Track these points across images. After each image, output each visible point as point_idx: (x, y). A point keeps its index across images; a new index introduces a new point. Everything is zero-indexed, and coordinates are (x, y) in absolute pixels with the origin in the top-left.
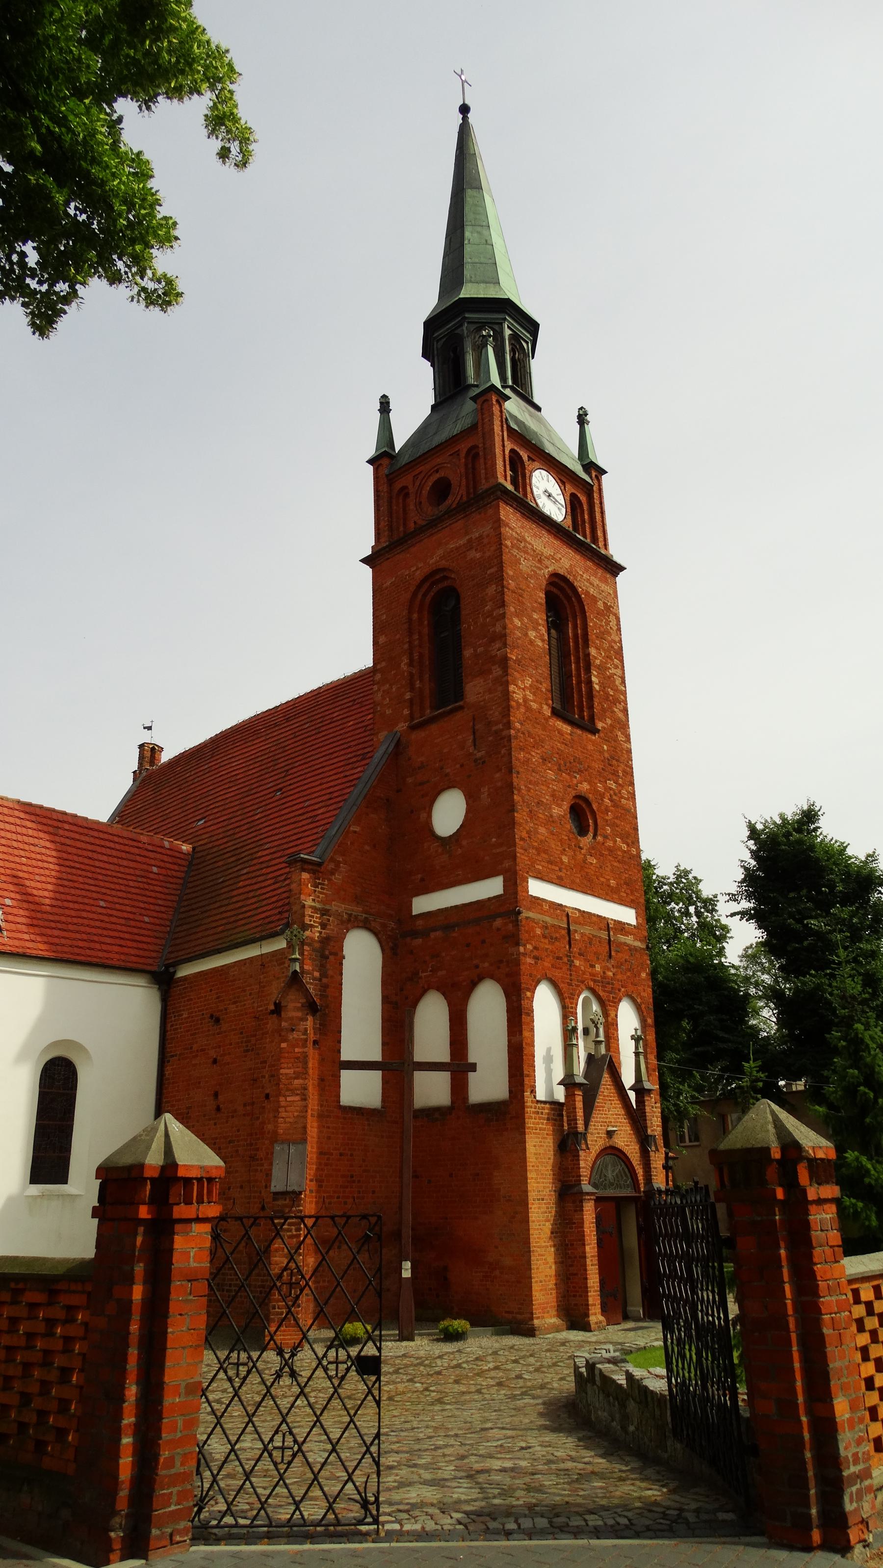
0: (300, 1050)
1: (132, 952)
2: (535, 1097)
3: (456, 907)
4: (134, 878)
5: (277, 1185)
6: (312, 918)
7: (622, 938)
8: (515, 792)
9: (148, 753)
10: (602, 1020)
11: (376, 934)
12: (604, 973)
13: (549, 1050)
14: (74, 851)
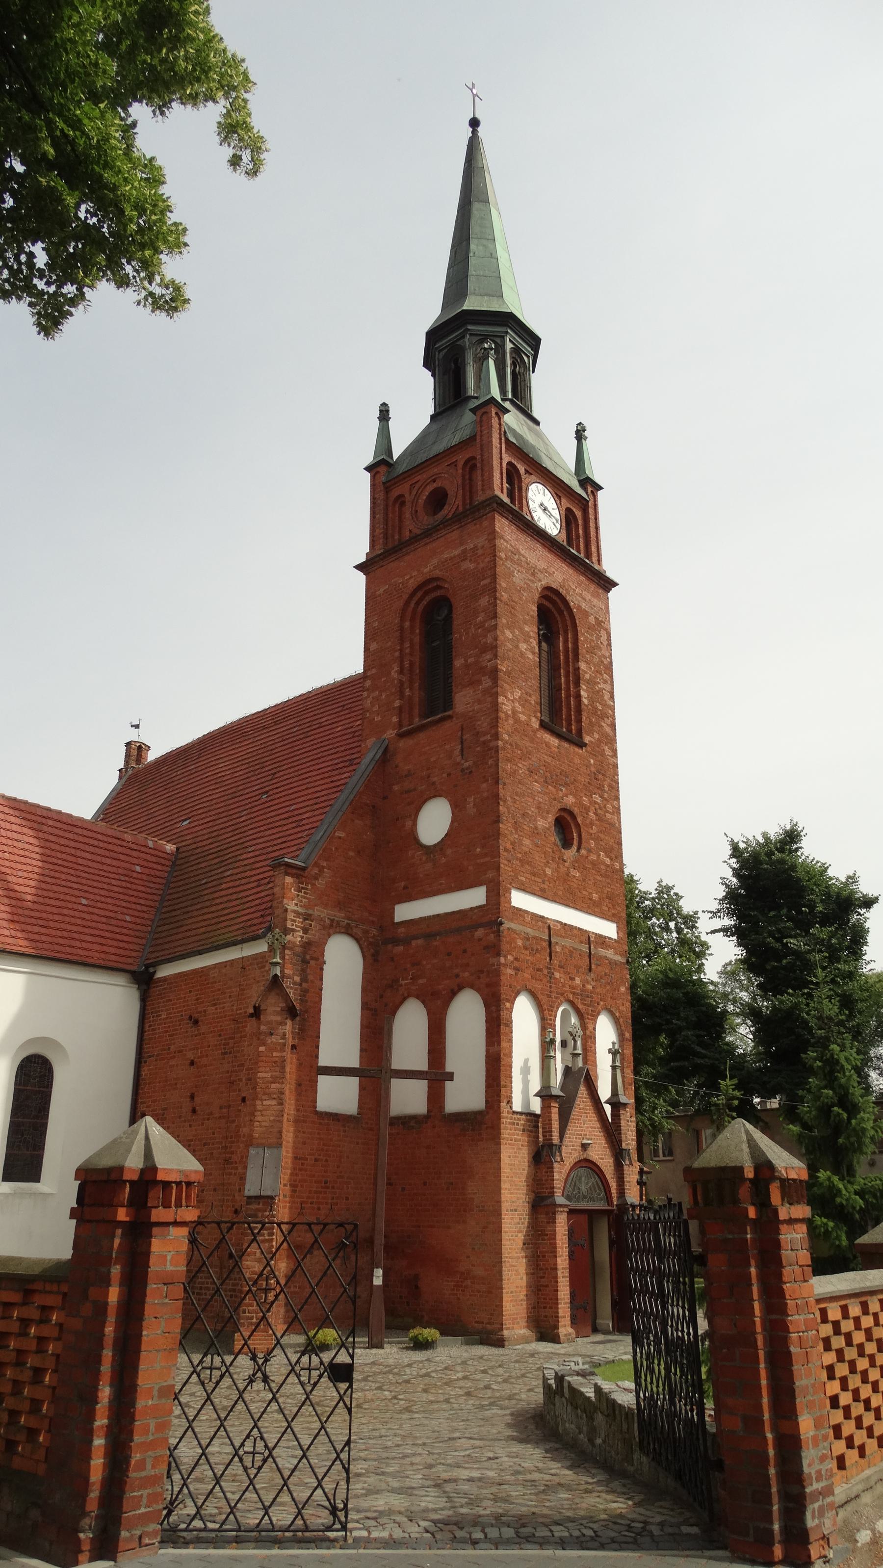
0: (278, 1054)
1: (112, 950)
2: (511, 1108)
3: (438, 915)
4: (117, 877)
5: (251, 1189)
6: (294, 922)
7: (603, 952)
8: (501, 803)
10: (580, 1033)
11: (357, 940)
12: (584, 986)
13: (526, 1061)
14: (57, 847)
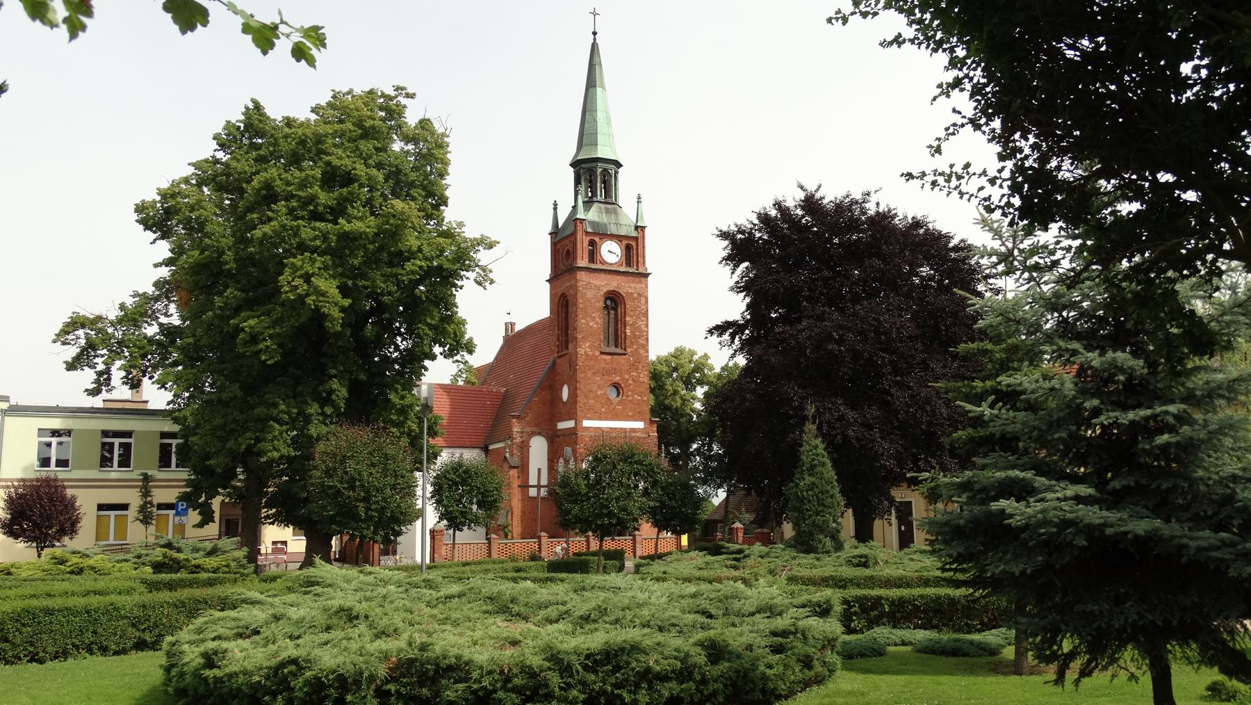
9: (509, 326)
